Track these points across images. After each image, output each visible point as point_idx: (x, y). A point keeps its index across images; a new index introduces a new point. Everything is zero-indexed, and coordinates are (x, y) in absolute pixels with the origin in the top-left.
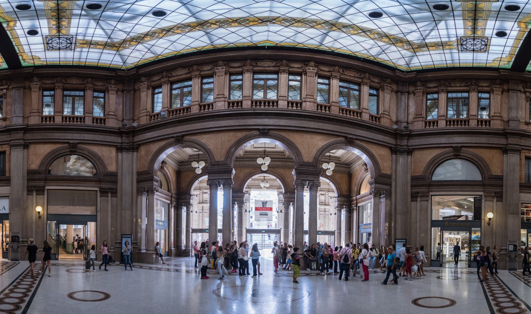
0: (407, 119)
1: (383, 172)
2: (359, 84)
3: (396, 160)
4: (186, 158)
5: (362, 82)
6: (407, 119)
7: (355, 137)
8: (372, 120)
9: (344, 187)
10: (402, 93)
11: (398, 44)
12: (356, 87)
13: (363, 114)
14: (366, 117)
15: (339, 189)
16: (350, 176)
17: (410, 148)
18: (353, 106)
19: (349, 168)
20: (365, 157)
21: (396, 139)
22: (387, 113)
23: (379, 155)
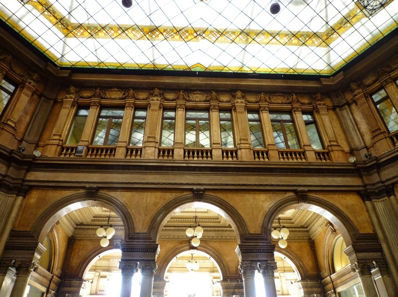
0: (364, 143)
1: (361, 232)
2: (290, 112)
3: (374, 208)
4: (88, 219)
6: (364, 143)
7: (306, 189)
8: (321, 159)
9: (308, 263)
10: (341, 107)
11: (308, 42)
12: (287, 117)
13: (306, 152)
14: (311, 157)
15: (301, 268)
16: (312, 245)
17: (386, 184)
19: (308, 231)
20: (328, 216)
21: (361, 177)
23: (347, 207)
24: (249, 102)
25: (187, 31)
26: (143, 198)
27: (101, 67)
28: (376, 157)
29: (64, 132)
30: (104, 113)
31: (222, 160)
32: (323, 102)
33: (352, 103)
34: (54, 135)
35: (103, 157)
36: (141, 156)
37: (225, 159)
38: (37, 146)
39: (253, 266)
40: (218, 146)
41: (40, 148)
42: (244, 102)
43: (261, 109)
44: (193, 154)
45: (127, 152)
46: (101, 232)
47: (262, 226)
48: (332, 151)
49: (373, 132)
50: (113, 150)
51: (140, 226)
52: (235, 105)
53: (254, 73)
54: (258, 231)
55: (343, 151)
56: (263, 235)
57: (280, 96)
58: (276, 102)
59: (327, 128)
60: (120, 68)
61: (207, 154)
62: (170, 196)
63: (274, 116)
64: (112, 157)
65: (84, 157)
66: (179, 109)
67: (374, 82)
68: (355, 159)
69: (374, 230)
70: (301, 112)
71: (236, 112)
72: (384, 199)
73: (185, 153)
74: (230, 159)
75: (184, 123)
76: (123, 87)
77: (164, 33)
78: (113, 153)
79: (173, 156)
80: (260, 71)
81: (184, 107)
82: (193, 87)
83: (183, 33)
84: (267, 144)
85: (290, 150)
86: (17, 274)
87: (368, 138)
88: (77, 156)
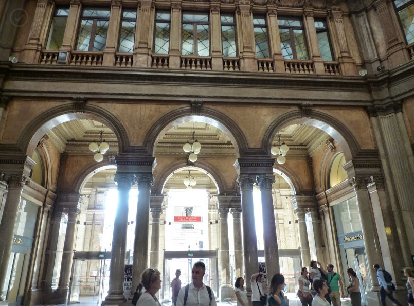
0: (378, 55)
1: (362, 148)
2: (300, 18)
4: (80, 136)
5: (304, 12)
7: (311, 103)
8: (330, 72)
10: (357, 13)
12: (297, 23)
14: (320, 68)
17: (395, 99)
18: (301, 55)
20: (331, 131)
21: (370, 92)
22: (346, 55)
23: (351, 123)
24: (255, 4)
26: (137, 111)
28: (388, 70)
29: (42, 35)
30: (87, 13)
31: (222, 70)
32: (338, 7)
33: (370, 9)
34: (31, 39)
35: (89, 64)
36: (132, 64)
37: (226, 69)
38: (13, 52)
39: (251, 178)
40: (218, 54)
41: (17, 54)
42: (250, 3)
43: (269, 12)
44: (191, 63)
45: (116, 59)
46: (93, 148)
47: (263, 141)
48: (343, 63)
49: (390, 43)
50: (99, 57)
51: (135, 140)
52: (239, 7)
54: (258, 145)
55: (354, 63)
56: (263, 150)
58: (285, 4)
59: (339, 38)
61: (206, 63)
62: (166, 109)
63: (283, 22)
64: (99, 65)
65: (67, 64)
66: (174, 10)
68: (366, 72)
69: (376, 147)
70: (313, 18)
71: (240, 15)
72: (390, 115)
73: (181, 62)
74: (231, 70)
75: (180, 27)
78: (100, 60)
79: (168, 65)
81: (180, 7)
84: (273, 53)
85: (297, 61)
86: (9, 188)
87: (382, 50)
88: (59, 63)
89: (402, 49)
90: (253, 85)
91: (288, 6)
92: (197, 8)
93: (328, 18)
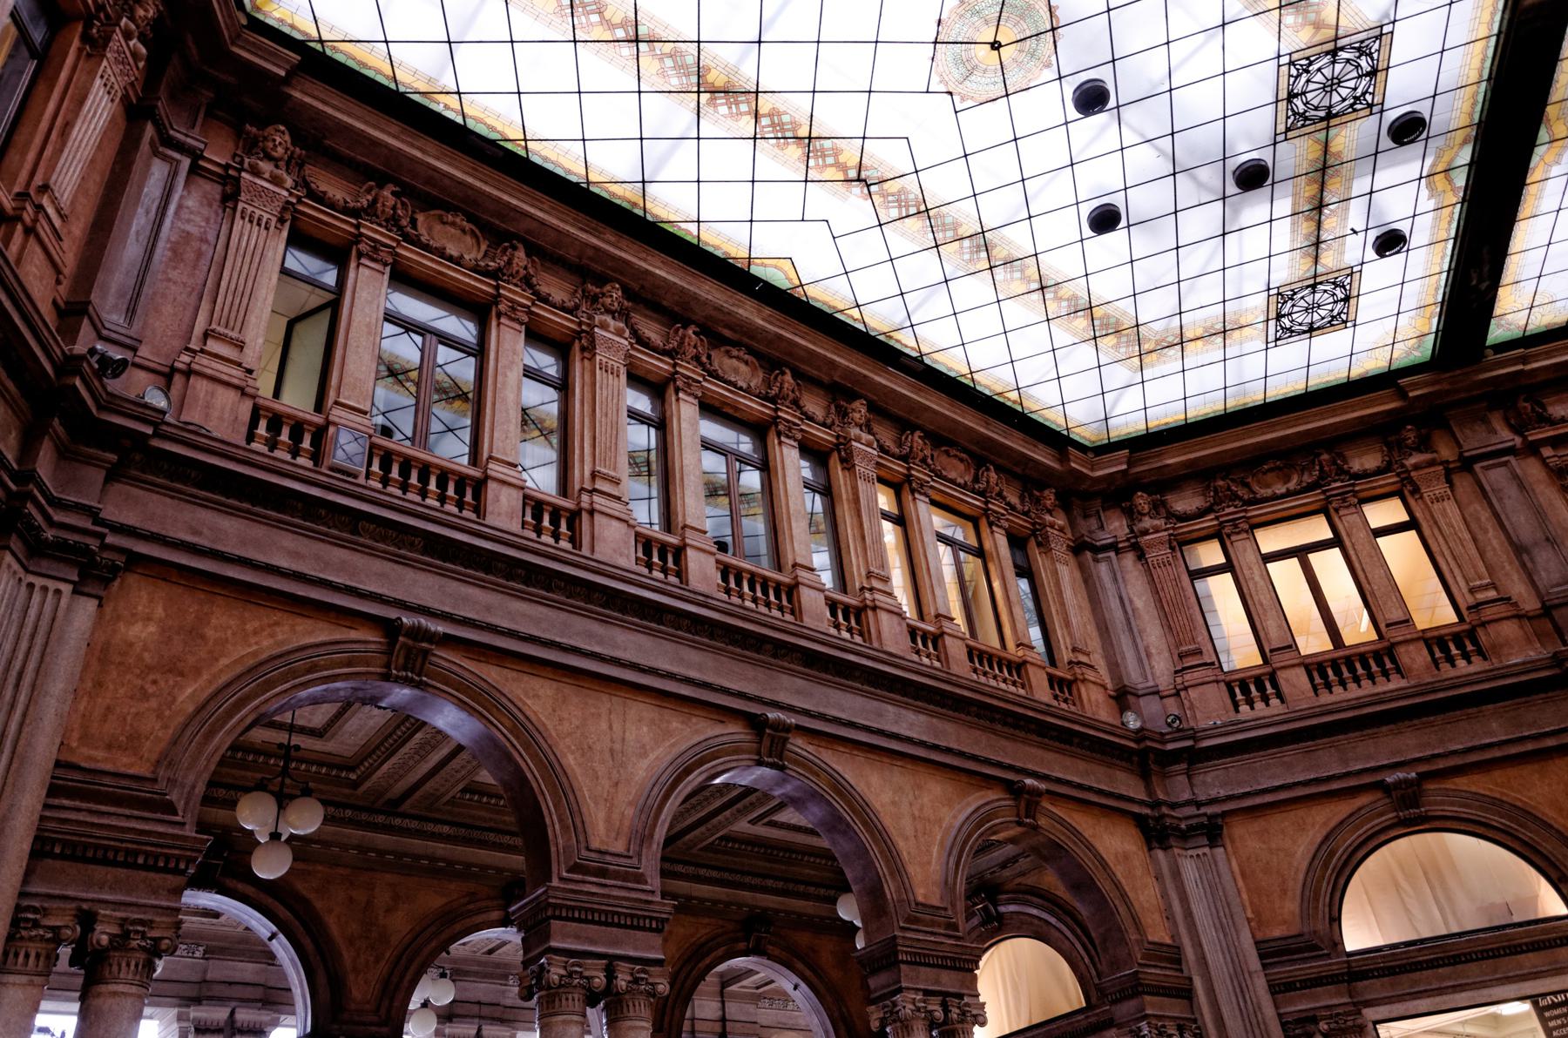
3: (1177, 874)
21: (1145, 776)
25: (836, 152)
27: (439, 108)
53: (919, 360)
55: (1104, 687)
57: (962, 460)
60: (509, 146)
67: (1201, 513)
69: (1175, 936)
72: (1200, 851)
76: (495, 229)
77: (765, 121)
80: (936, 361)
82: (728, 326)
83: (823, 150)
89: (1217, 682)
90: (944, 711)
91: (953, 481)
92: (736, 409)
93: (1032, 544)
